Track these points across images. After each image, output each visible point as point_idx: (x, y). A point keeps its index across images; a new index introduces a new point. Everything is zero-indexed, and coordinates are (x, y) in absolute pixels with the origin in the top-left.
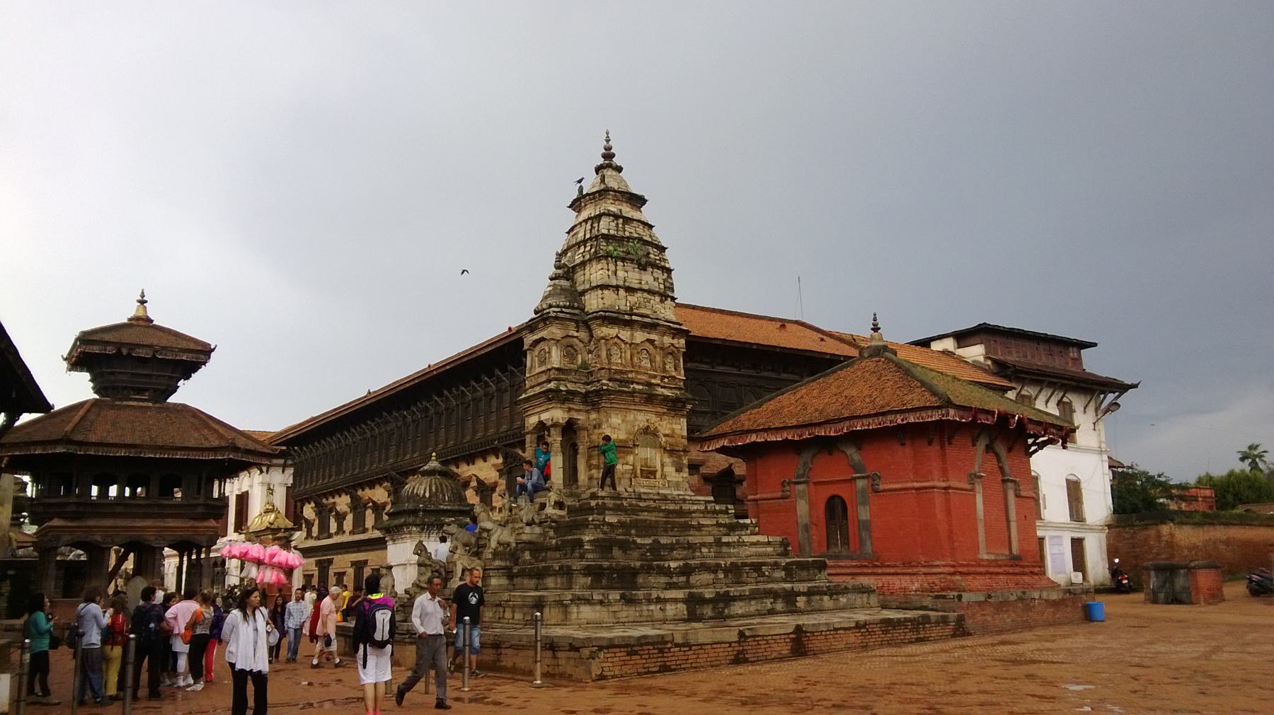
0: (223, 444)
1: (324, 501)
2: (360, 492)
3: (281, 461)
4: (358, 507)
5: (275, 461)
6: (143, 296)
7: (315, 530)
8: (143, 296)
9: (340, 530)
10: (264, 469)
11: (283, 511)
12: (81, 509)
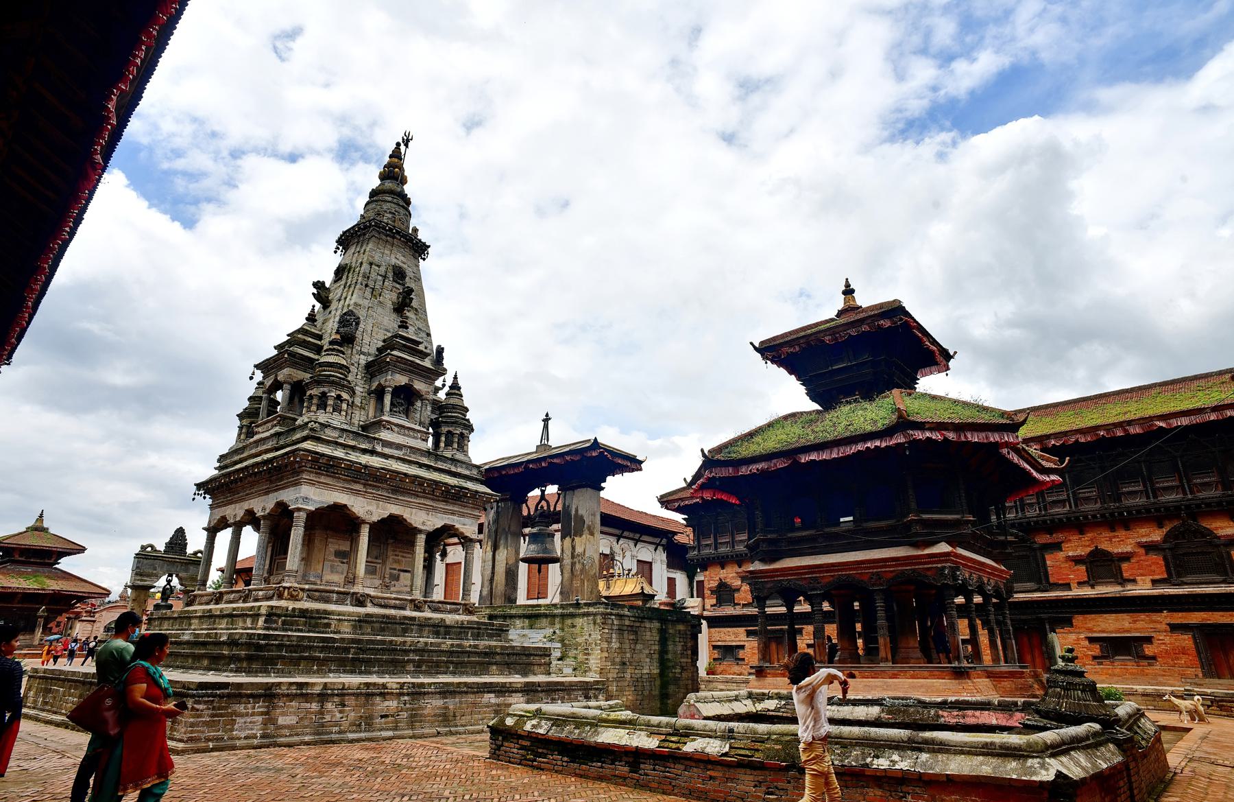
6: (847, 285)
8: (847, 285)
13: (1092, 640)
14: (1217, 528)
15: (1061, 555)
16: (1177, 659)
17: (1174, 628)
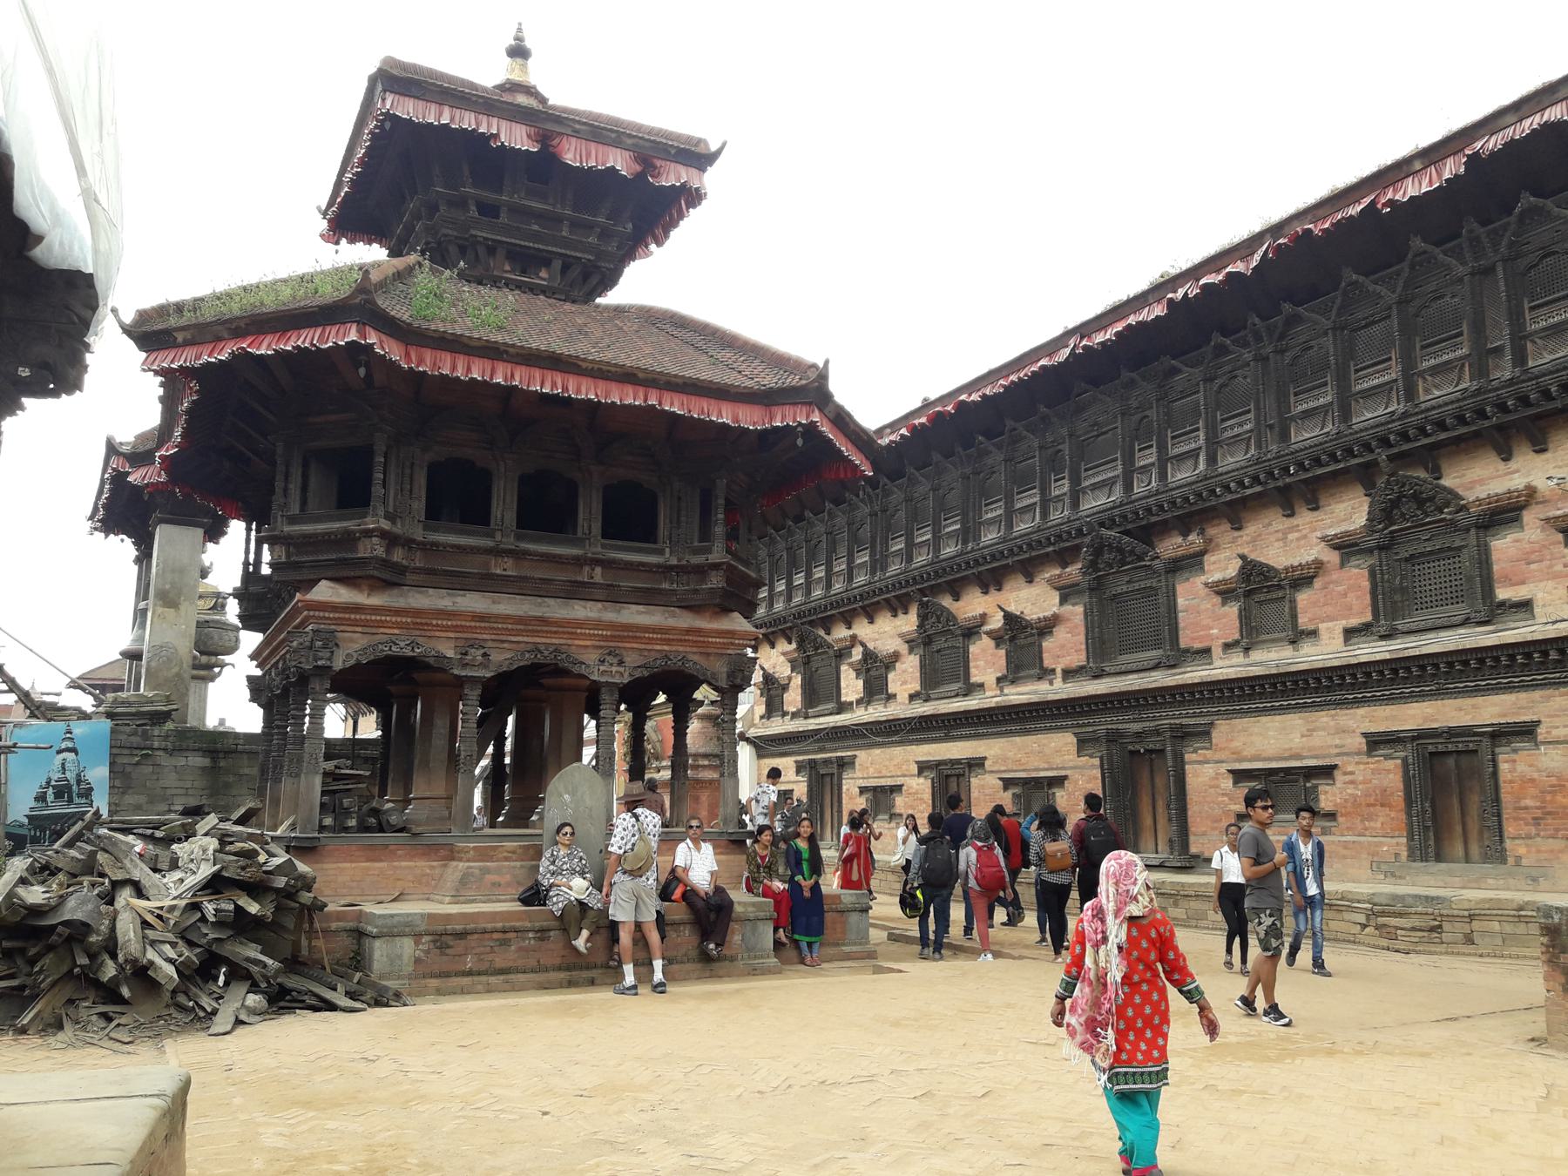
0: (794, 381)
1: (822, 633)
2: (947, 601)
7: (793, 698)
12: (398, 556)
13: (1239, 776)
14: (1471, 485)
15: (1199, 581)
16: (1370, 819)
17: (1377, 742)
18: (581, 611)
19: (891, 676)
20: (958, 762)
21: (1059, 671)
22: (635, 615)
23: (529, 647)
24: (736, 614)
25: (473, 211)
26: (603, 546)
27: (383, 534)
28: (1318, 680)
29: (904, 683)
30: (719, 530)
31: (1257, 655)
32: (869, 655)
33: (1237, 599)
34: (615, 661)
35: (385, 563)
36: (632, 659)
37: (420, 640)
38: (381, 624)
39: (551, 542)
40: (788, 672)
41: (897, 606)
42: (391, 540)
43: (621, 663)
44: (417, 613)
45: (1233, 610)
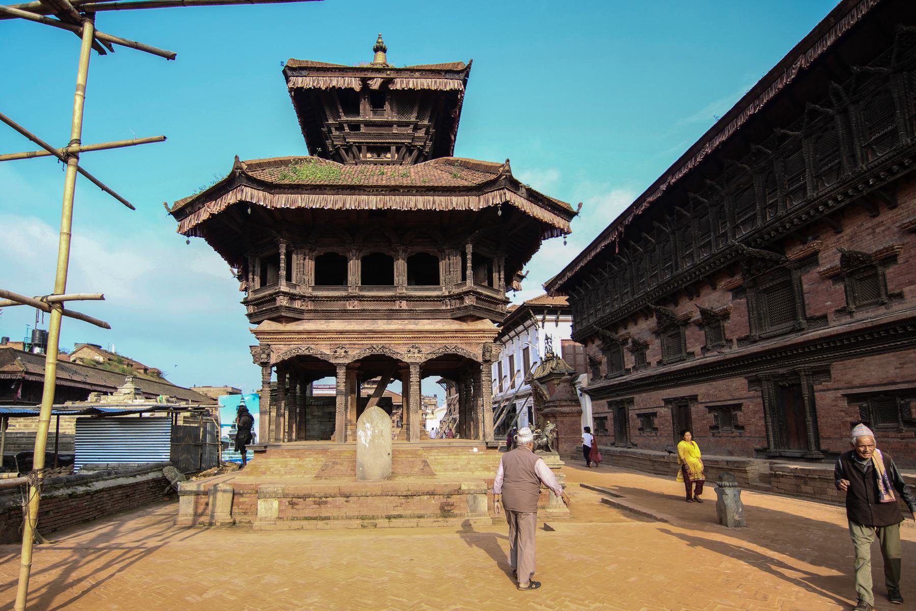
2: (671, 308)
3: (553, 317)
4: (671, 329)
5: (548, 317)
9: (642, 362)
10: (540, 324)
11: (560, 355)
12: (297, 304)
18: (395, 325)
19: (648, 352)
20: (683, 398)
21: (735, 341)
22: (426, 325)
23: (369, 346)
24: (488, 320)
25: (347, 130)
26: (407, 289)
27: (285, 294)
28: (905, 328)
29: (654, 356)
30: (469, 272)
31: (858, 316)
32: (634, 342)
33: (843, 280)
34: (416, 351)
35: (288, 309)
36: (426, 350)
37: (312, 346)
38: (291, 339)
39: (384, 290)
40: (601, 356)
41: (646, 313)
42: (292, 297)
43: (419, 352)
44: (309, 332)
45: (840, 287)
